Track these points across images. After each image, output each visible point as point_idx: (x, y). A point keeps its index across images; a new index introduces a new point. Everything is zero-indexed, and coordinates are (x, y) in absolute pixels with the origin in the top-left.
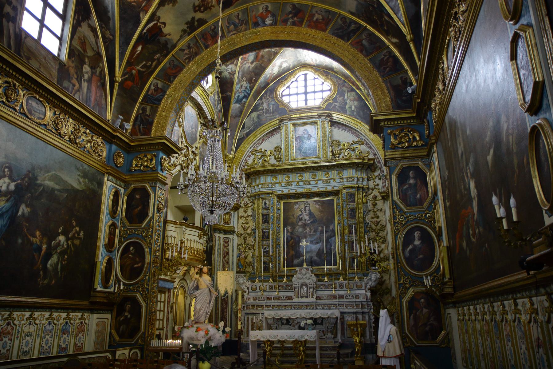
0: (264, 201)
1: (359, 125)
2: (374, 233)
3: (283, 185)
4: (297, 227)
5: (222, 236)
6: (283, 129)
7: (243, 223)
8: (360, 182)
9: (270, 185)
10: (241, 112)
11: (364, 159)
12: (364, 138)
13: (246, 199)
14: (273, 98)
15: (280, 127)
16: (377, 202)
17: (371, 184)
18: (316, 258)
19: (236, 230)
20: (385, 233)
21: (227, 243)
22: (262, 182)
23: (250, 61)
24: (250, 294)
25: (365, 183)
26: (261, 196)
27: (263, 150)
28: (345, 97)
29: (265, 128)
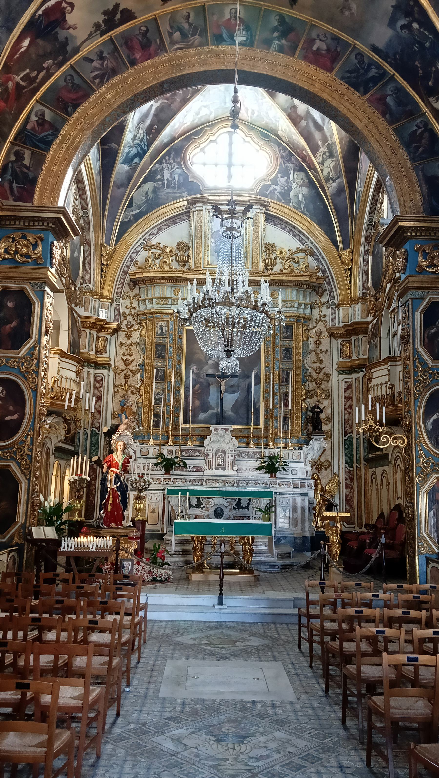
0: (160, 324)
1: (307, 224)
2: (314, 383)
4: (206, 367)
5: (92, 371)
6: (194, 216)
7: (124, 355)
8: (301, 310)
9: (170, 301)
10: (129, 179)
11: (311, 277)
12: (311, 245)
13: (130, 318)
14: (179, 164)
15: (188, 212)
16: (322, 340)
17: (316, 313)
18: (230, 413)
19: (112, 363)
20: (329, 385)
21: (99, 382)
22: (157, 295)
24: (139, 460)
25: (308, 311)
27: (161, 246)
28: (289, 178)
29: (165, 210)
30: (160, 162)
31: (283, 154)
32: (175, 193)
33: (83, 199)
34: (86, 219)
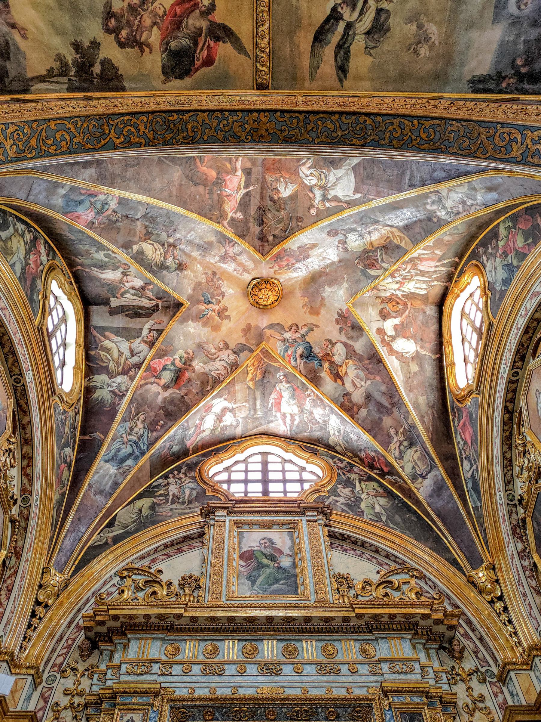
1: (397, 540)
3: (196, 669)
6: (211, 533)
9: (156, 668)
14: (193, 478)
22: (132, 654)
23: (162, 382)
26: (119, 700)
28: (354, 487)
29: (165, 529)
30: (166, 477)
31: (341, 465)
32: (184, 509)
33: (27, 475)
34: (25, 511)
